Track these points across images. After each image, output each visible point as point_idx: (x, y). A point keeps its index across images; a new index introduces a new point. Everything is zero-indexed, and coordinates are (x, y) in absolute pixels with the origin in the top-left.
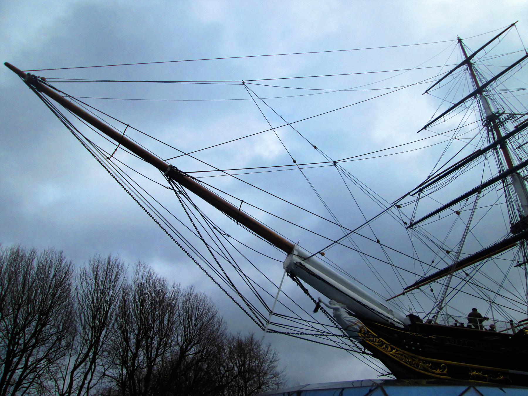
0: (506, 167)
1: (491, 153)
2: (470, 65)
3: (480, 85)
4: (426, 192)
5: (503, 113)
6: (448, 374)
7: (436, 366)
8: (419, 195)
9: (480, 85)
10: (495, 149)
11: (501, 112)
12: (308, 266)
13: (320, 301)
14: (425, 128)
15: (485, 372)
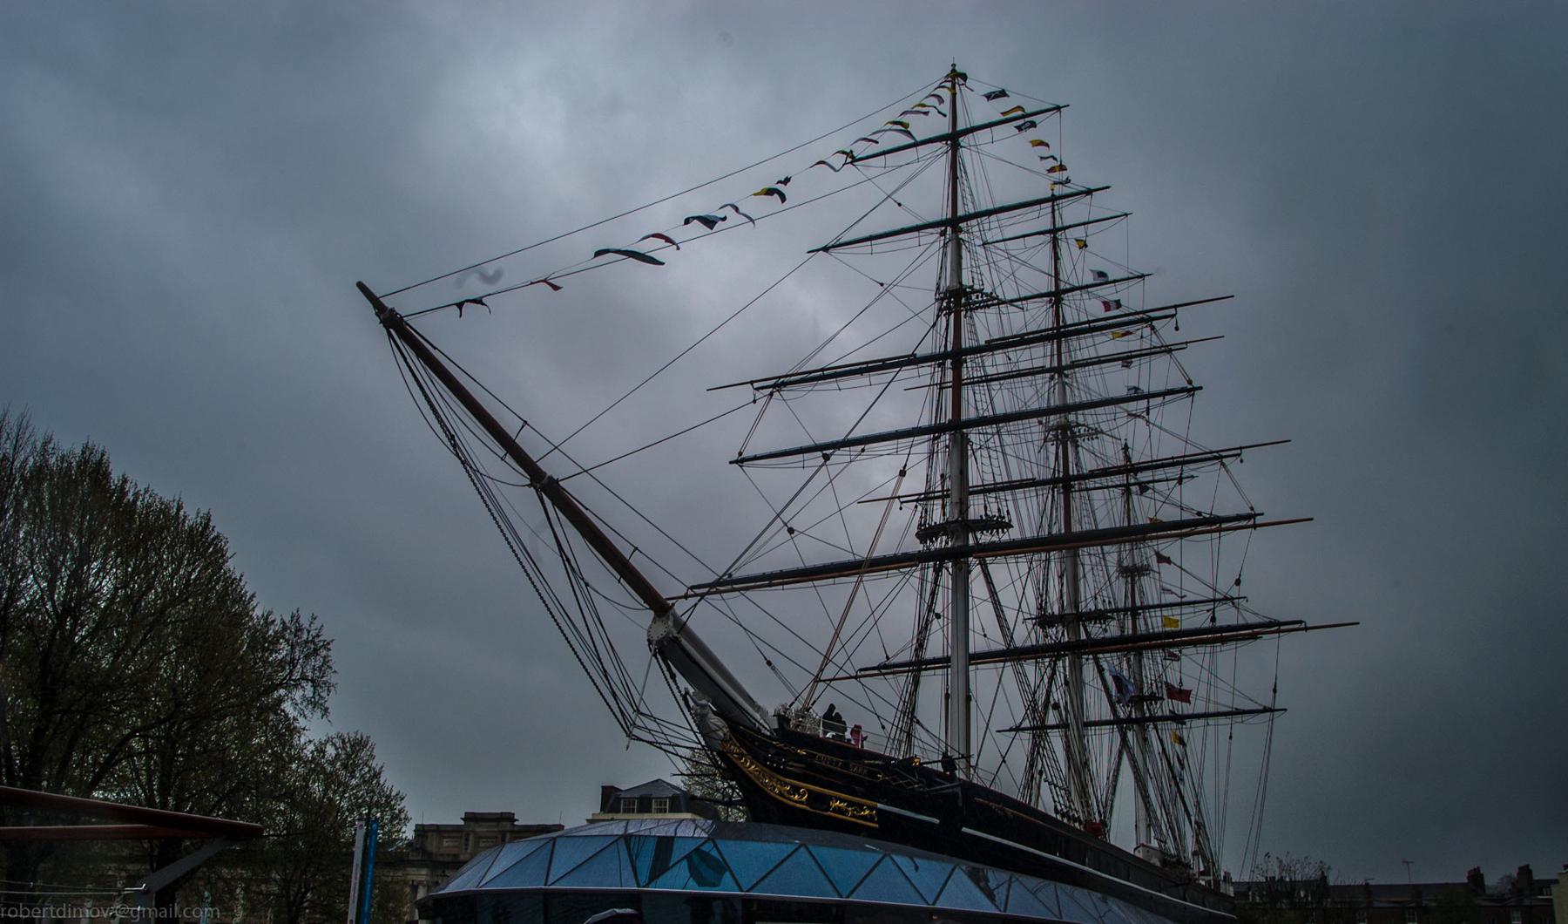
0: (948, 415)
1: (929, 370)
2: (955, 147)
3: (960, 213)
4: (787, 393)
5: (981, 291)
6: (808, 802)
7: (795, 790)
8: (771, 394)
9: (960, 213)
10: (942, 365)
11: (977, 287)
12: (684, 642)
13: (687, 693)
14: (826, 249)
15: (851, 804)
